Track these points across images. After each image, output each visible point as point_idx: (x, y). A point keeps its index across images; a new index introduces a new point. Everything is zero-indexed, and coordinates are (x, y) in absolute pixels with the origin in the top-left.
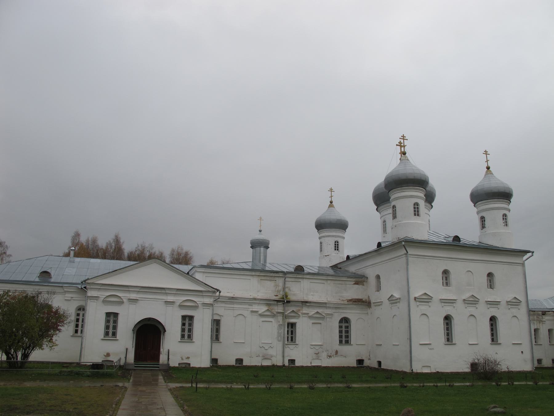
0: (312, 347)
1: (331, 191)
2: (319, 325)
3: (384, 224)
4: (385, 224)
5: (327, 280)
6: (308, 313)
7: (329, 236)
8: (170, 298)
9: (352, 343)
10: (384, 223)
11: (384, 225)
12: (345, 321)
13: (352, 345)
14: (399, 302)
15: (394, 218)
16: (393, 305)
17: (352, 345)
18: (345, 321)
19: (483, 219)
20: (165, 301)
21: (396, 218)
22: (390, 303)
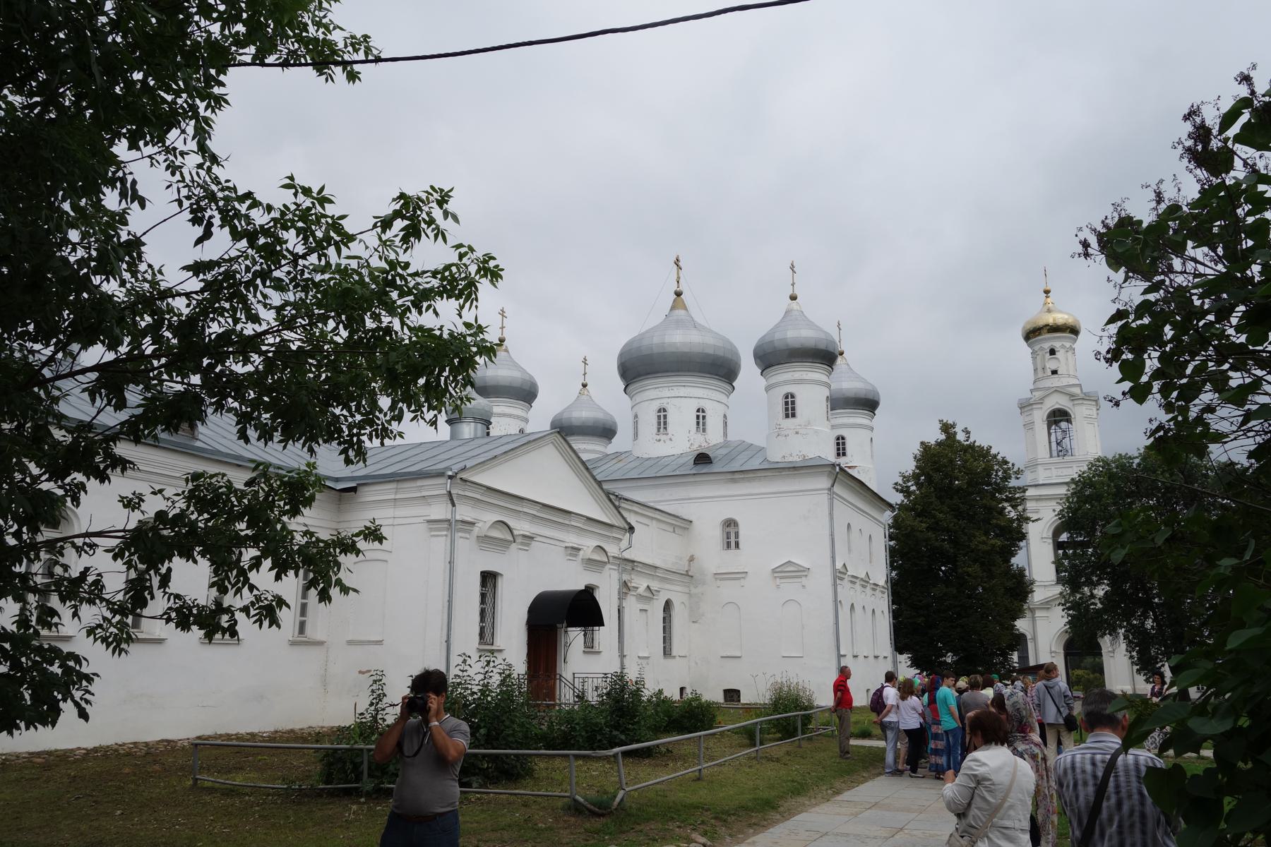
0: (640, 661)
1: (503, 316)
2: (644, 613)
3: (662, 414)
4: (665, 417)
5: (653, 518)
6: (637, 588)
7: (510, 416)
8: (572, 539)
9: (674, 653)
10: (659, 411)
11: (659, 417)
12: (668, 606)
13: (674, 657)
14: (806, 576)
15: (787, 416)
16: (783, 581)
17: (674, 657)
18: (668, 606)
19: (841, 441)
20: (566, 547)
21: (794, 415)
22: (776, 577)
